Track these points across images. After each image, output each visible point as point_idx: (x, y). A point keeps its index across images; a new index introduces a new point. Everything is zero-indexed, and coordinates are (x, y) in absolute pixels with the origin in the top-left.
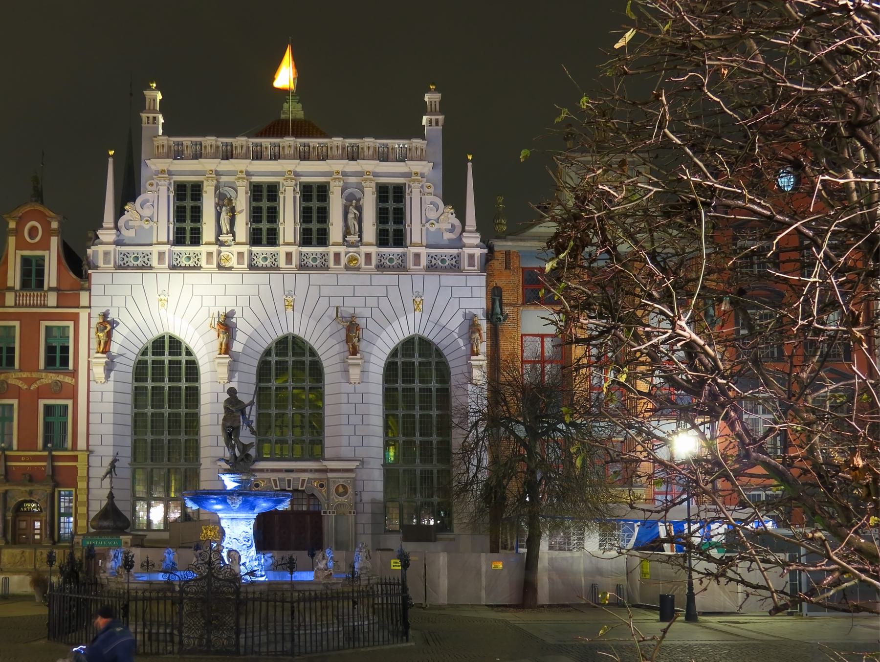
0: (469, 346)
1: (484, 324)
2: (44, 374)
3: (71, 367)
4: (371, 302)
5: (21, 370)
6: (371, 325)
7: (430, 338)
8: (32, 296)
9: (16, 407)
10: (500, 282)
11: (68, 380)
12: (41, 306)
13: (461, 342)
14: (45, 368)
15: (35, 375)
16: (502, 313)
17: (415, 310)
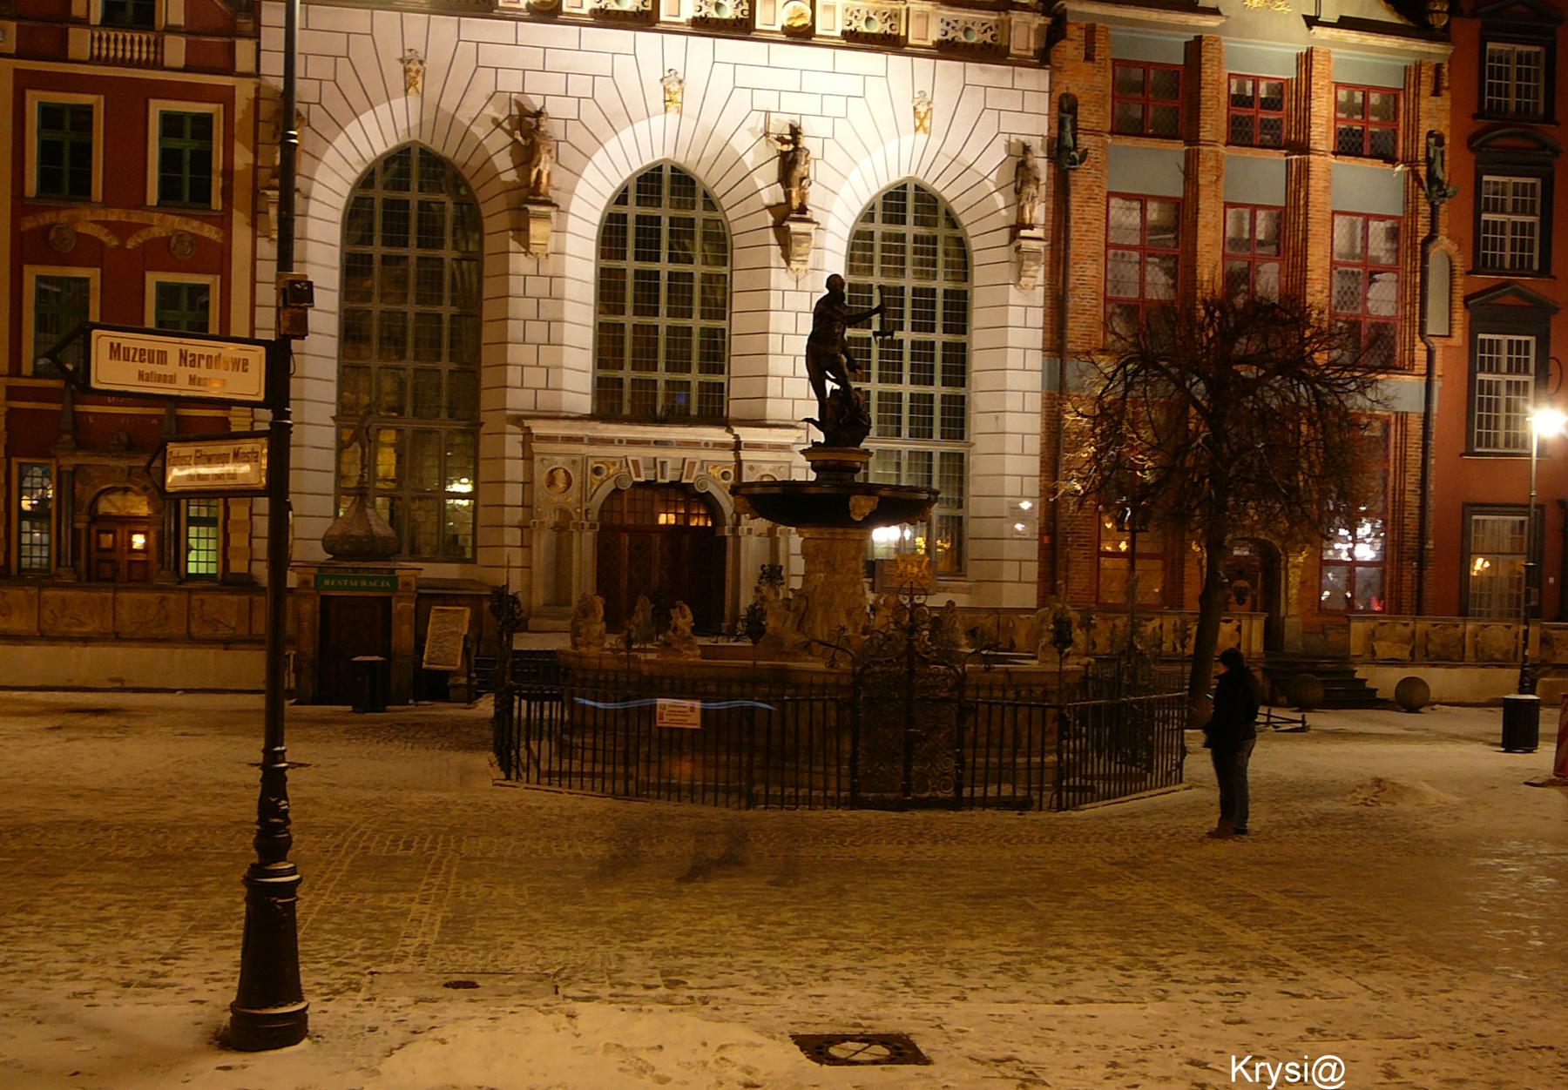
0: (1014, 209)
1: (1041, 165)
2: (156, 217)
3: (217, 202)
4: (834, 106)
5: (107, 204)
6: (833, 153)
7: (938, 187)
8: (135, 43)
9: (95, 283)
10: (1074, 85)
11: (210, 232)
12: (147, 65)
13: (1000, 200)
14: (159, 204)
15: (136, 217)
16: (1075, 148)
17: (917, 129)
